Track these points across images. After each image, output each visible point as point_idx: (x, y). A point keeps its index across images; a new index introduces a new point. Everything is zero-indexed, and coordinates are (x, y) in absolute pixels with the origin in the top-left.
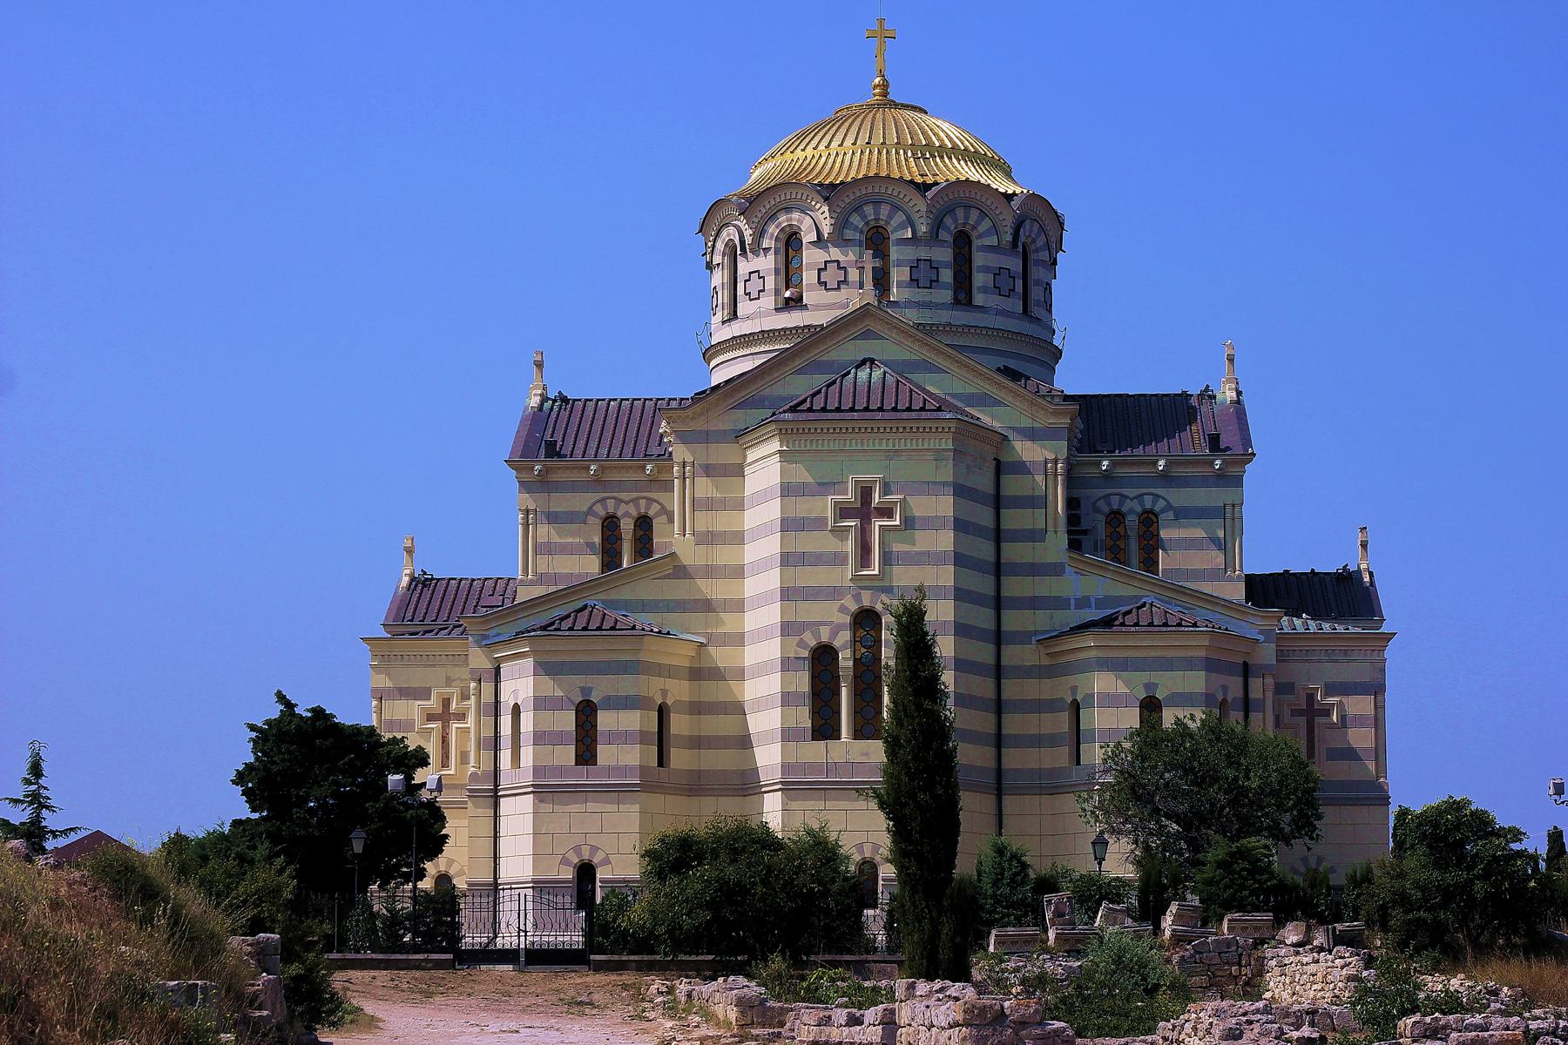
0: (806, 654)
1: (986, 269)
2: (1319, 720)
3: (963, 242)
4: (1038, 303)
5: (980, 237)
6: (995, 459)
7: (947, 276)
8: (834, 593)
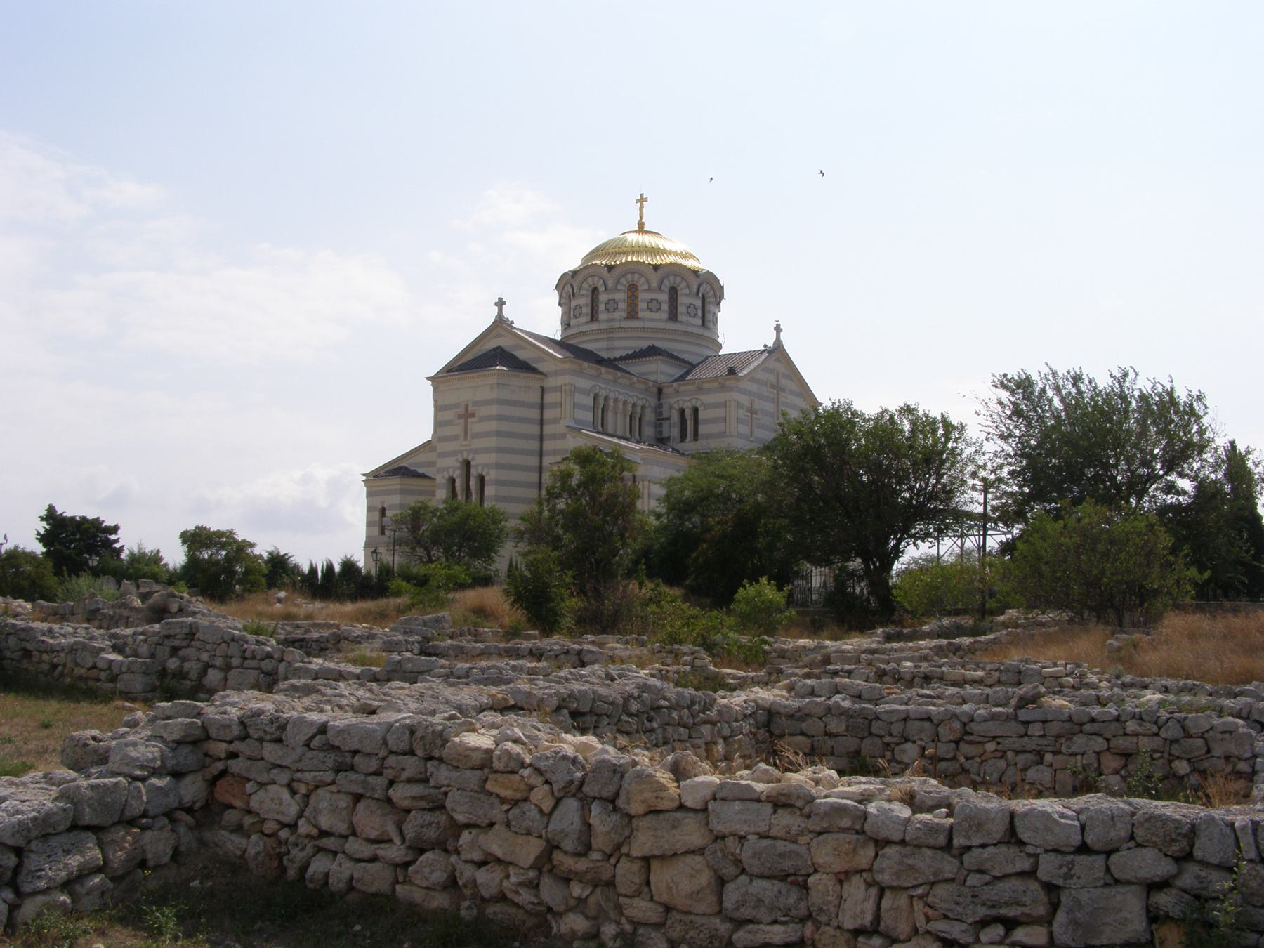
0: (444, 481)
3: (633, 288)
4: (681, 314)
7: (622, 306)
8: (453, 454)
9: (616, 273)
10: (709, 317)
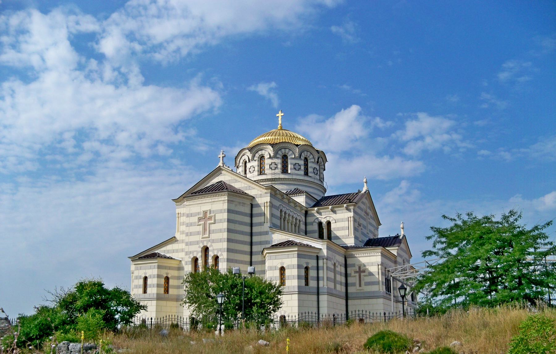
1: (291, 164)
2: (362, 274)
3: (285, 158)
4: (311, 172)
5: (289, 156)
6: (251, 204)
7: (280, 166)
8: (197, 243)
9: (277, 147)
10: (322, 176)
